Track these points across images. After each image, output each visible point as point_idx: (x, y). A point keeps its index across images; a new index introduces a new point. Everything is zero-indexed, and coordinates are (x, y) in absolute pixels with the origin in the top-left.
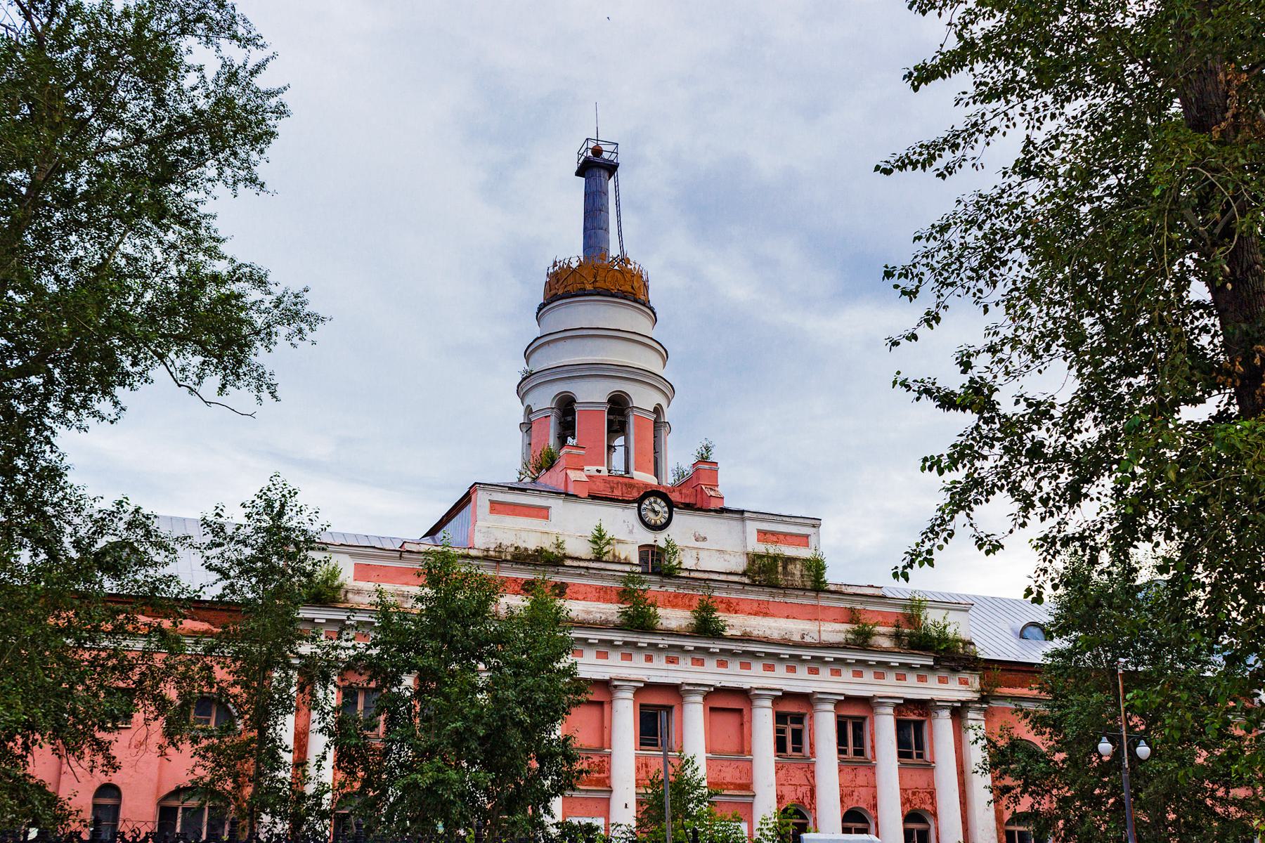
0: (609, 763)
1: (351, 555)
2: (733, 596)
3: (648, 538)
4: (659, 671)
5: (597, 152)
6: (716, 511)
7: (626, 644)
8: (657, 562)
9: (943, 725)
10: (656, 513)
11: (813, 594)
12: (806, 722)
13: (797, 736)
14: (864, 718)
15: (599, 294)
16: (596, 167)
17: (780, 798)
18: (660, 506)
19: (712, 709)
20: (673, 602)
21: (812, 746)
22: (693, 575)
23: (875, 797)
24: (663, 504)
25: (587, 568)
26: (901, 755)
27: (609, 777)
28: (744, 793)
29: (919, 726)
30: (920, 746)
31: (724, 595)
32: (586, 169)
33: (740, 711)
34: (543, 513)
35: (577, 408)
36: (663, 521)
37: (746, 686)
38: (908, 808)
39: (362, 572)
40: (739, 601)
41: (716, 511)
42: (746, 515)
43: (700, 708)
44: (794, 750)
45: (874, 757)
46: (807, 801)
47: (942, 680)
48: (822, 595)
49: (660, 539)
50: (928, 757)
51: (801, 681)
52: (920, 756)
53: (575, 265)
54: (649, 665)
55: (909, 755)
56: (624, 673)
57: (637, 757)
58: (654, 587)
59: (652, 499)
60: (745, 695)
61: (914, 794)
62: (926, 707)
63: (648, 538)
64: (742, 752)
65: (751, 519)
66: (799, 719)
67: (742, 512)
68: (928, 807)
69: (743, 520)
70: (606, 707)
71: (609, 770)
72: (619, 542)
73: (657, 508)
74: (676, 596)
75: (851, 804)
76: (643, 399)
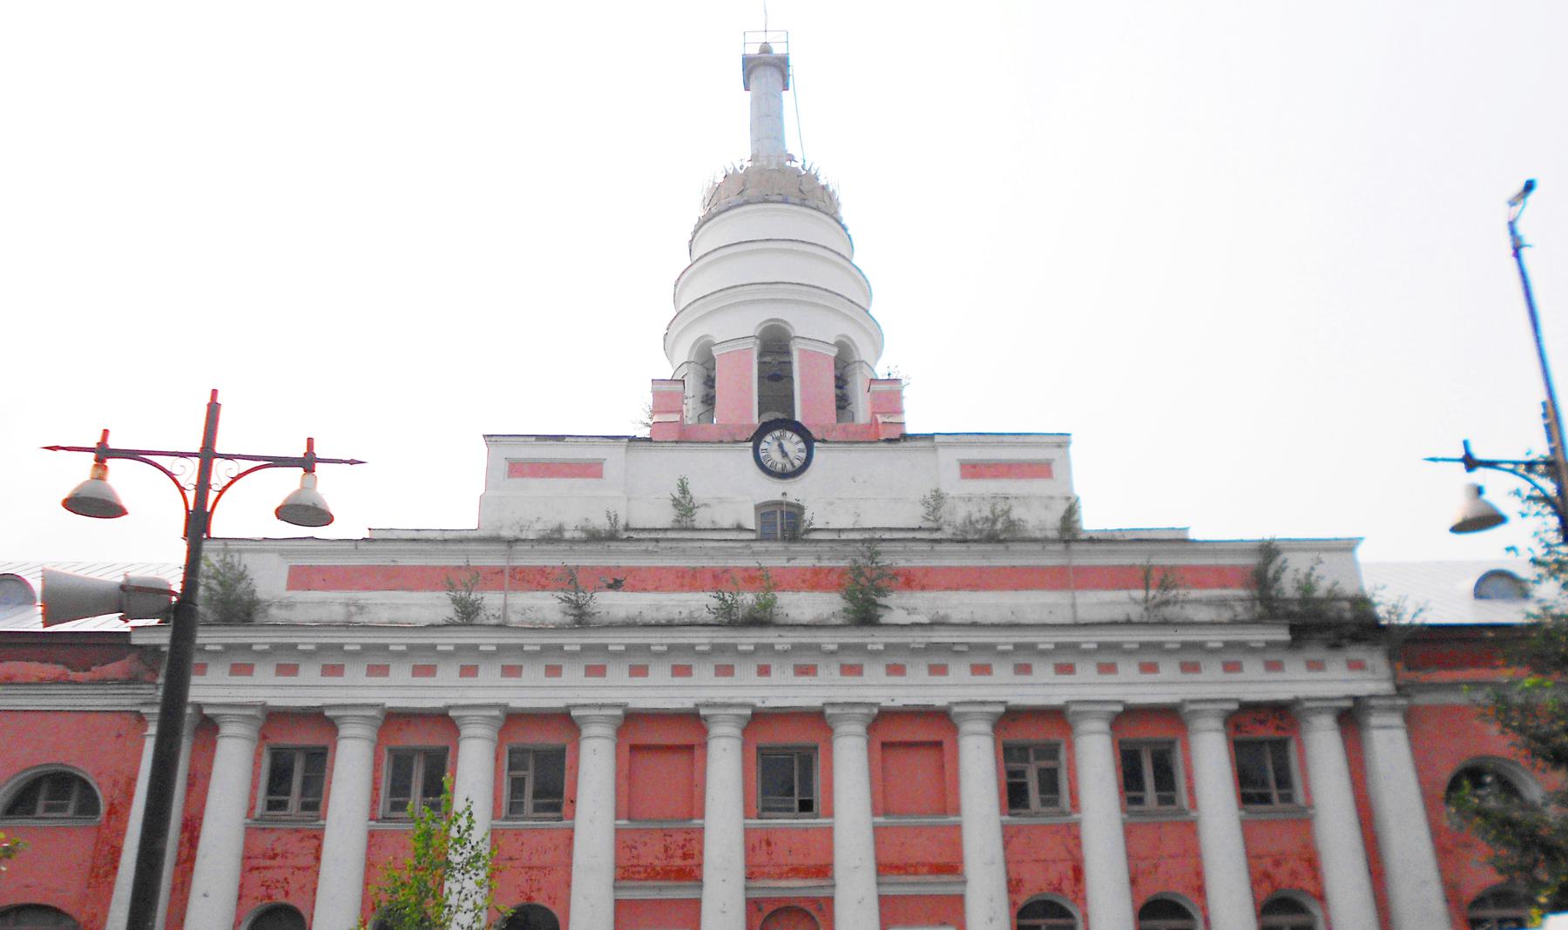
0: (701, 842)
1: (282, 553)
2: (917, 562)
3: (773, 490)
4: (785, 690)
5: (766, 49)
6: (889, 441)
7: (718, 649)
8: (784, 523)
9: (1323, 749)
10: (785, 454)
11: (1060, 547)
12: (1063, 756)
13: (1050, 783)
14: (1172, 743)
15: (747, 203)
16: (766, 69)
17: (1014, 886)
18: (793, 444)
19: (886, 746)
20: (815, 580)
21: (1074, 797)
22: (844, 536)
23: (1199, 874)
24: (796, 438)
25: (657, 540)
26: (1245, 799)
27: (700, 865)
28: (945, 878)
29: (1280, 747)
30: (1284, 781)
31: (902, 563)
32: (750, 66)
33: (937, 745)
34: (591, 470)
35: (716, 352)
36: (798, 463)
37: (940, 702)
38: (1266, 890)
39: (301, 578)
40: (928, 571)
41: (889, 441)
42: (937, 439)
43: (861, 743)
44: (1044, 803)
45: (1194, 805)
46: (1067, 886)
47: (1315, 666)
48: (1075, 547)
49: (794, 491)
50: (1300, 798)
51: (1041, 689)
52: (1287, 798)
53: (720, 179)
54: (764, 680)
55: (1265, 799)
56: (720, 695)
57: (748, 832)
58: (775, 558)
59: (777, 433)
60: (942, 718)
61: (1277, 863)
62: (1284, 714)
63: (773, 490)
64: (944, 812)
65: (949, 445)
66: (1051, 751)
67: (930, 437)
68: (1308, 884)
69: (935, 448)
70: (697, 752)
71: (701, 853)
72: (721, 500)
73: (787, 446)
74: (816, 571)
75: (1154, 888)
76: (814, 332)
